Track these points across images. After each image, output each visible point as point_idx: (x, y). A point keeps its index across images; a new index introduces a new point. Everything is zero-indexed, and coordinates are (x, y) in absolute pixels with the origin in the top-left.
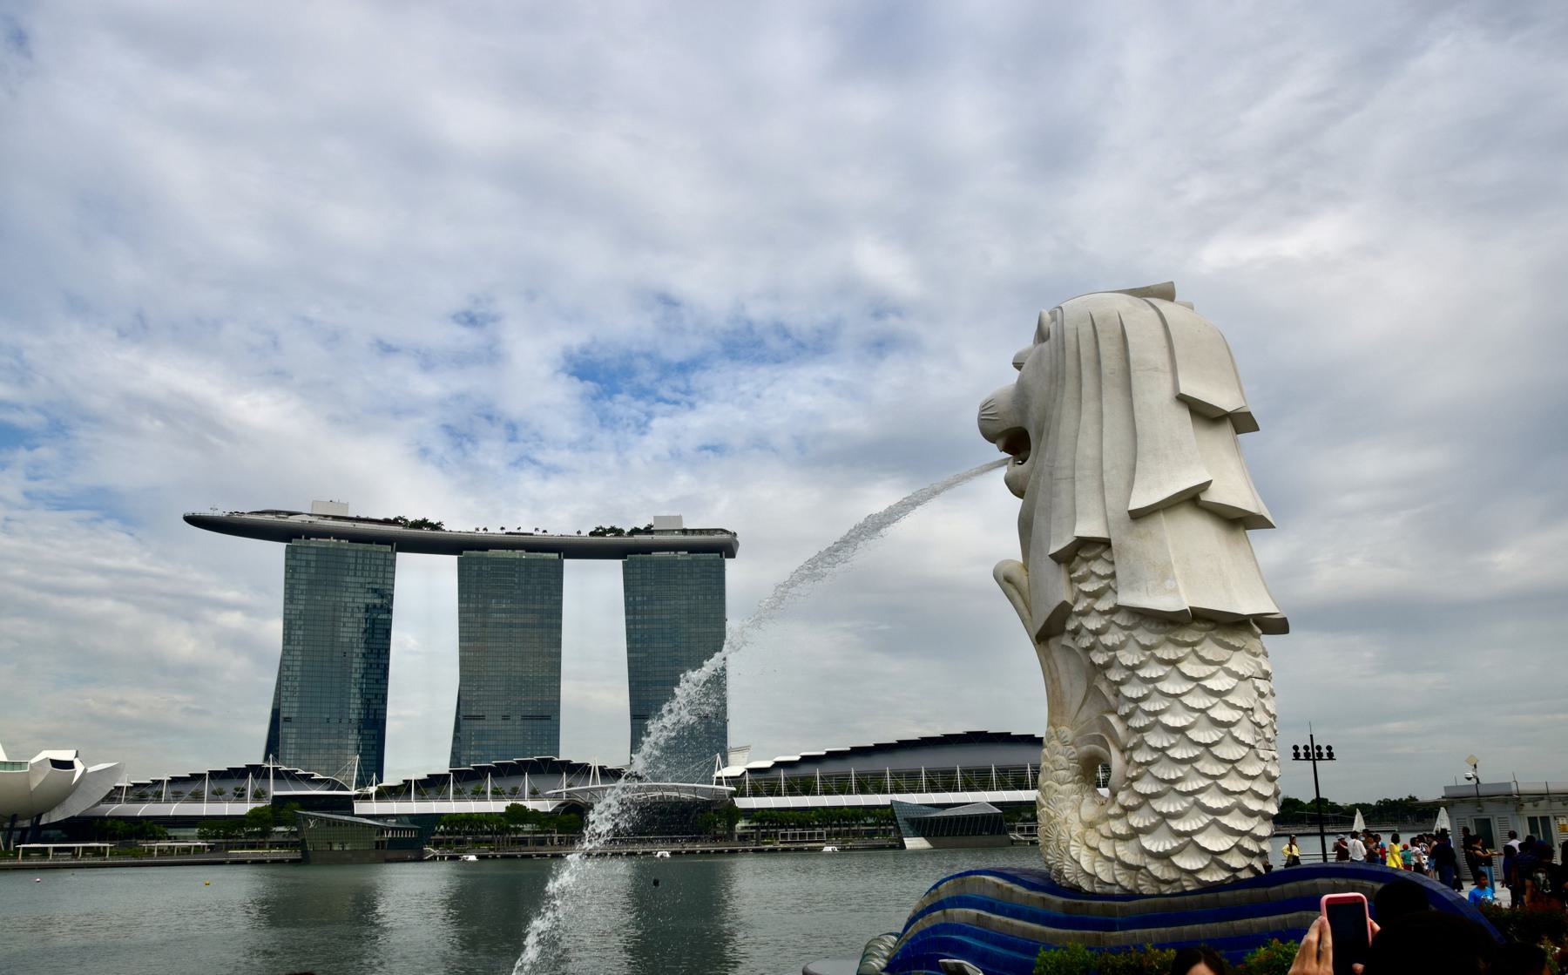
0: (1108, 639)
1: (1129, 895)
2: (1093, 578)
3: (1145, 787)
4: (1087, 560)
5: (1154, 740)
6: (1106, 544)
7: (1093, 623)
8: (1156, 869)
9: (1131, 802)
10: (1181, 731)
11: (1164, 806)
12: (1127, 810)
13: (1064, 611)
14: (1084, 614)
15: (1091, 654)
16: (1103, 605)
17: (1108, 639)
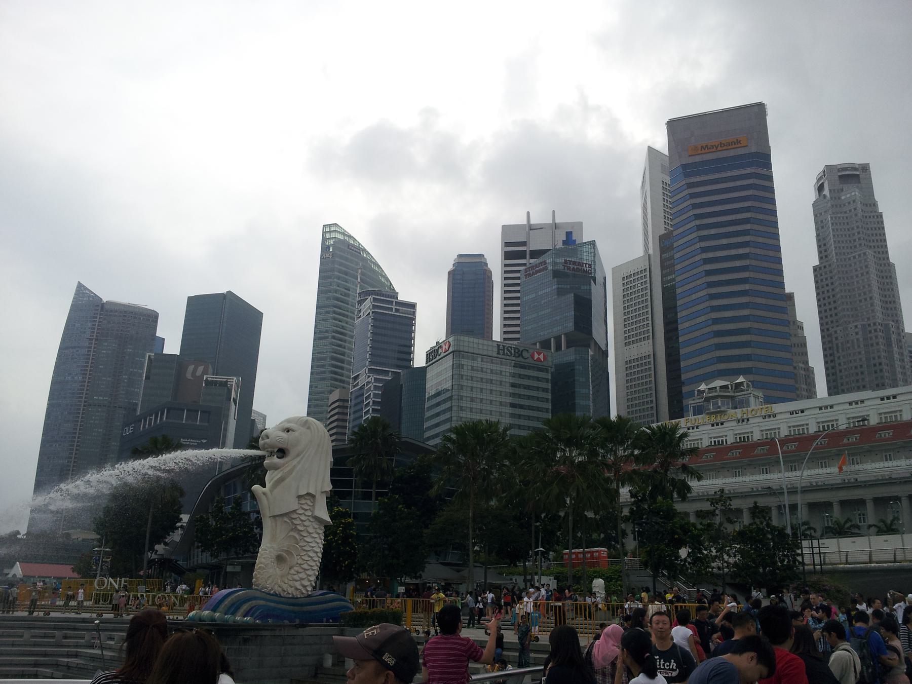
0: (305, 523)
1: (293, 598)
3: (306, 566)
5: (311, 554)
6: (313, 496)
7: (303, 518)
8: (304, 591)
9: (300, 570)
10: (317, 553)
11: (308, 572)
12: (298, 572)
13: (295, 511)
16: (309, 513)
17: (305, 523)
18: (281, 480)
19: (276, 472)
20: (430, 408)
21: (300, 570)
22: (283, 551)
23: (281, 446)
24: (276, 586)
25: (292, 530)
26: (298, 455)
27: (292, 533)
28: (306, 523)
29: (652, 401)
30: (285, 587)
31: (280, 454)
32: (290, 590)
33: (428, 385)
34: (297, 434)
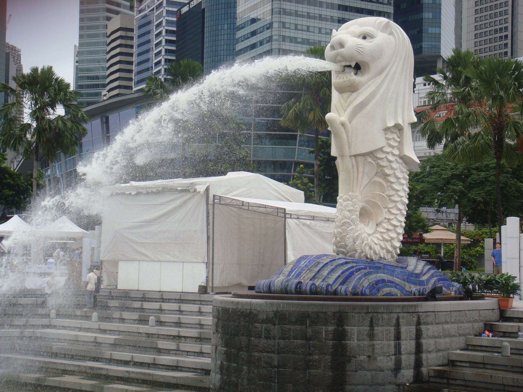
2: (392, 140)
4: (392, 132)
7: (391, 158)
9: (391, 228)
12: (388, 230)
13: (381, 149)
14: (388, 153)
15: (385, 169)
18: (362, 106)
19: (354, 94)
20: (245, 38)
21: (391, 228)
22: (368, 202)
23: (359, 58)
24: (367, 248)
25: (376, 174)
26: (381, 72)
27: (377, 179)
28: (395, 165)
29: (506, 28)
30: (377, 248)
31: (355, 72)
32: (383, 253)
33: (240, 9)
34: (376, 41)
